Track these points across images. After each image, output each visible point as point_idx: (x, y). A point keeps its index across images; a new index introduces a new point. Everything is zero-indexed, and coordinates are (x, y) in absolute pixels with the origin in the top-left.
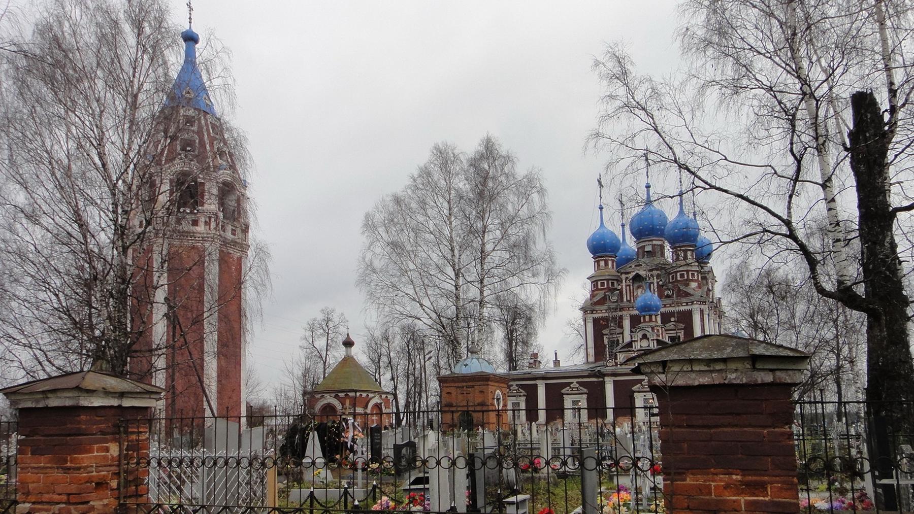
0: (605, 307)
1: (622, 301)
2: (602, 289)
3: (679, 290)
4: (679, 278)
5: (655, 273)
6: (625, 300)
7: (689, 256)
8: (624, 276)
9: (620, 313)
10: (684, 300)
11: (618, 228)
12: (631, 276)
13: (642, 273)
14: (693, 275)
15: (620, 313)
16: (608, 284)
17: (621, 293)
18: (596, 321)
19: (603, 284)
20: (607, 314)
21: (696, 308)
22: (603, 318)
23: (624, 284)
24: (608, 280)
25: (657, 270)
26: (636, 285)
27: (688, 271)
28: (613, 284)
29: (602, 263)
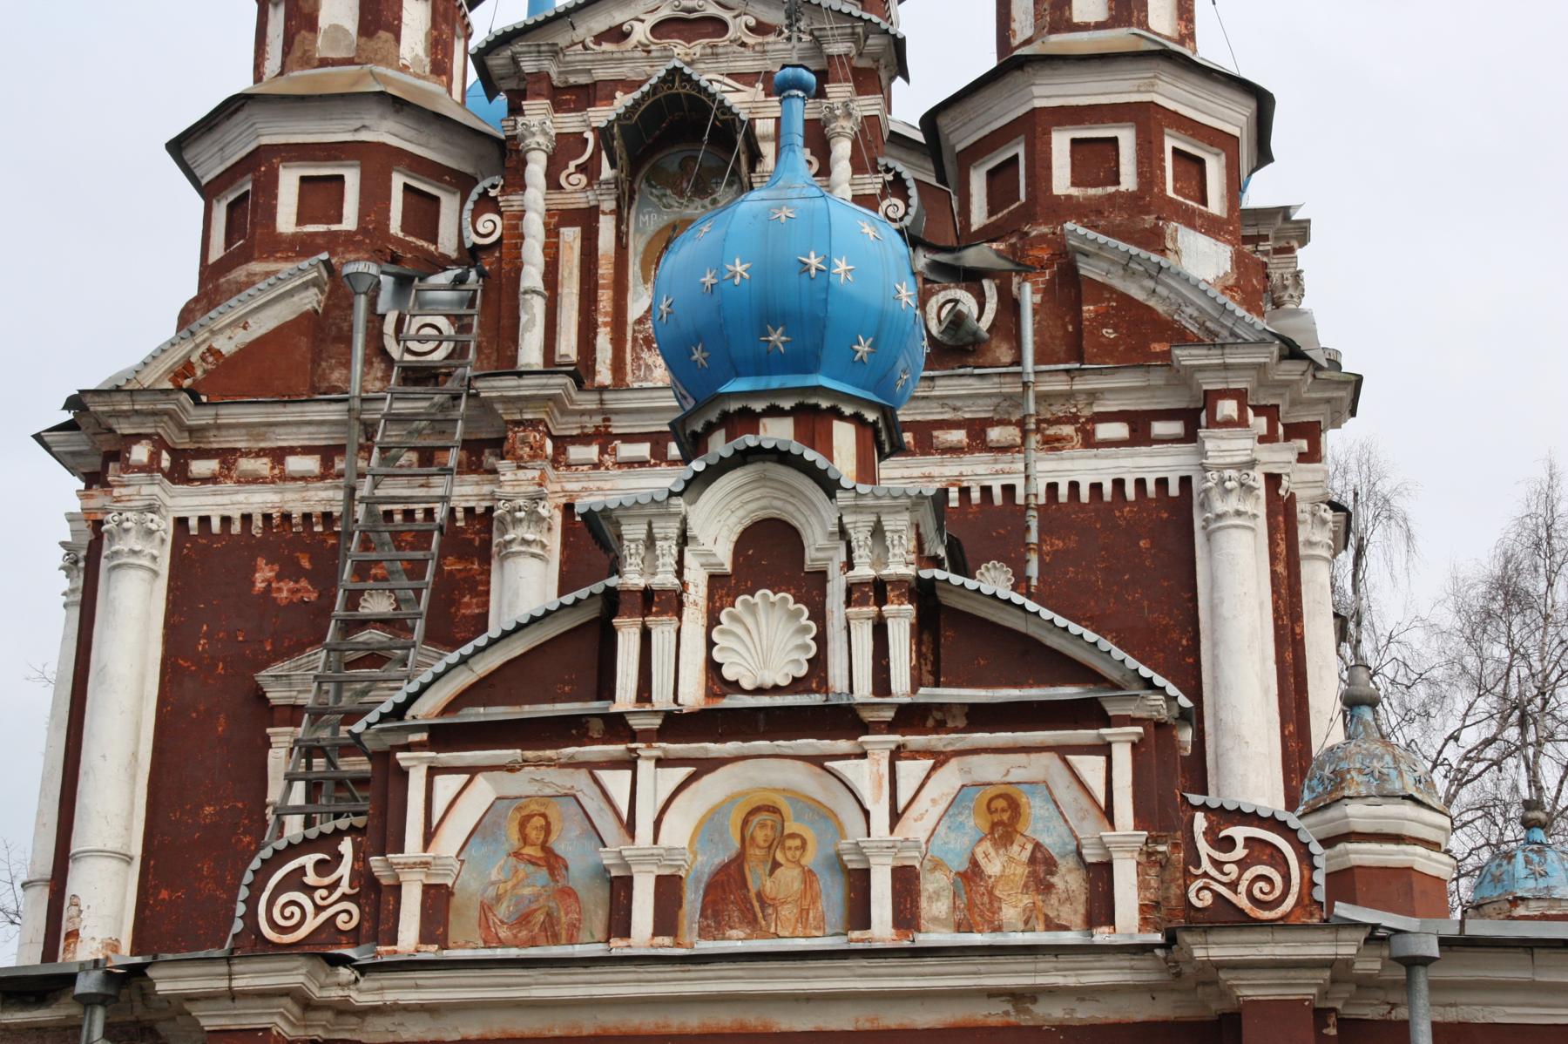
0: (319, 418)
1: (507, 365)
2: (302, 247)
3: (1068, 285)
4: (1061, 181)
6: (530, 352)
9: (467, 492)
10: (1122, 389)
15: (467, 492)
16: (375, 197)
18: (199, 560)
20: (324, 498)
22: (282, 537)
23: (535, 198)
24: (377, 161)
26: (646, 222)
27: (1149, 120)
28: (423, 212)
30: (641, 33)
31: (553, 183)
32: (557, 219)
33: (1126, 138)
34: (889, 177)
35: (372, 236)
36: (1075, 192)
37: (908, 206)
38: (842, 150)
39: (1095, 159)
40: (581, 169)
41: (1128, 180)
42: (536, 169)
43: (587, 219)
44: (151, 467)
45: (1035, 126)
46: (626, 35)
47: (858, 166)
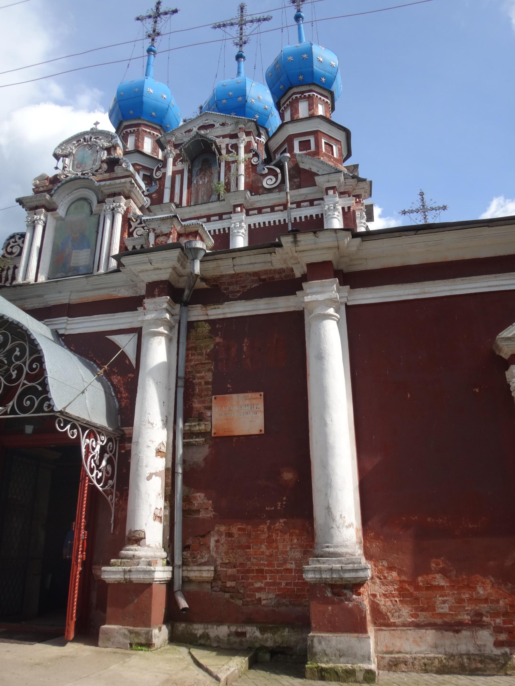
31: (174, 165)
32: (174, 173)
33: (312, 140)
34: (254, 153)
36: (301, 152)
37: (259, 158)
39: (305, 145)
40: (180, 161)
43: (181, 172)
46: (192, 130)
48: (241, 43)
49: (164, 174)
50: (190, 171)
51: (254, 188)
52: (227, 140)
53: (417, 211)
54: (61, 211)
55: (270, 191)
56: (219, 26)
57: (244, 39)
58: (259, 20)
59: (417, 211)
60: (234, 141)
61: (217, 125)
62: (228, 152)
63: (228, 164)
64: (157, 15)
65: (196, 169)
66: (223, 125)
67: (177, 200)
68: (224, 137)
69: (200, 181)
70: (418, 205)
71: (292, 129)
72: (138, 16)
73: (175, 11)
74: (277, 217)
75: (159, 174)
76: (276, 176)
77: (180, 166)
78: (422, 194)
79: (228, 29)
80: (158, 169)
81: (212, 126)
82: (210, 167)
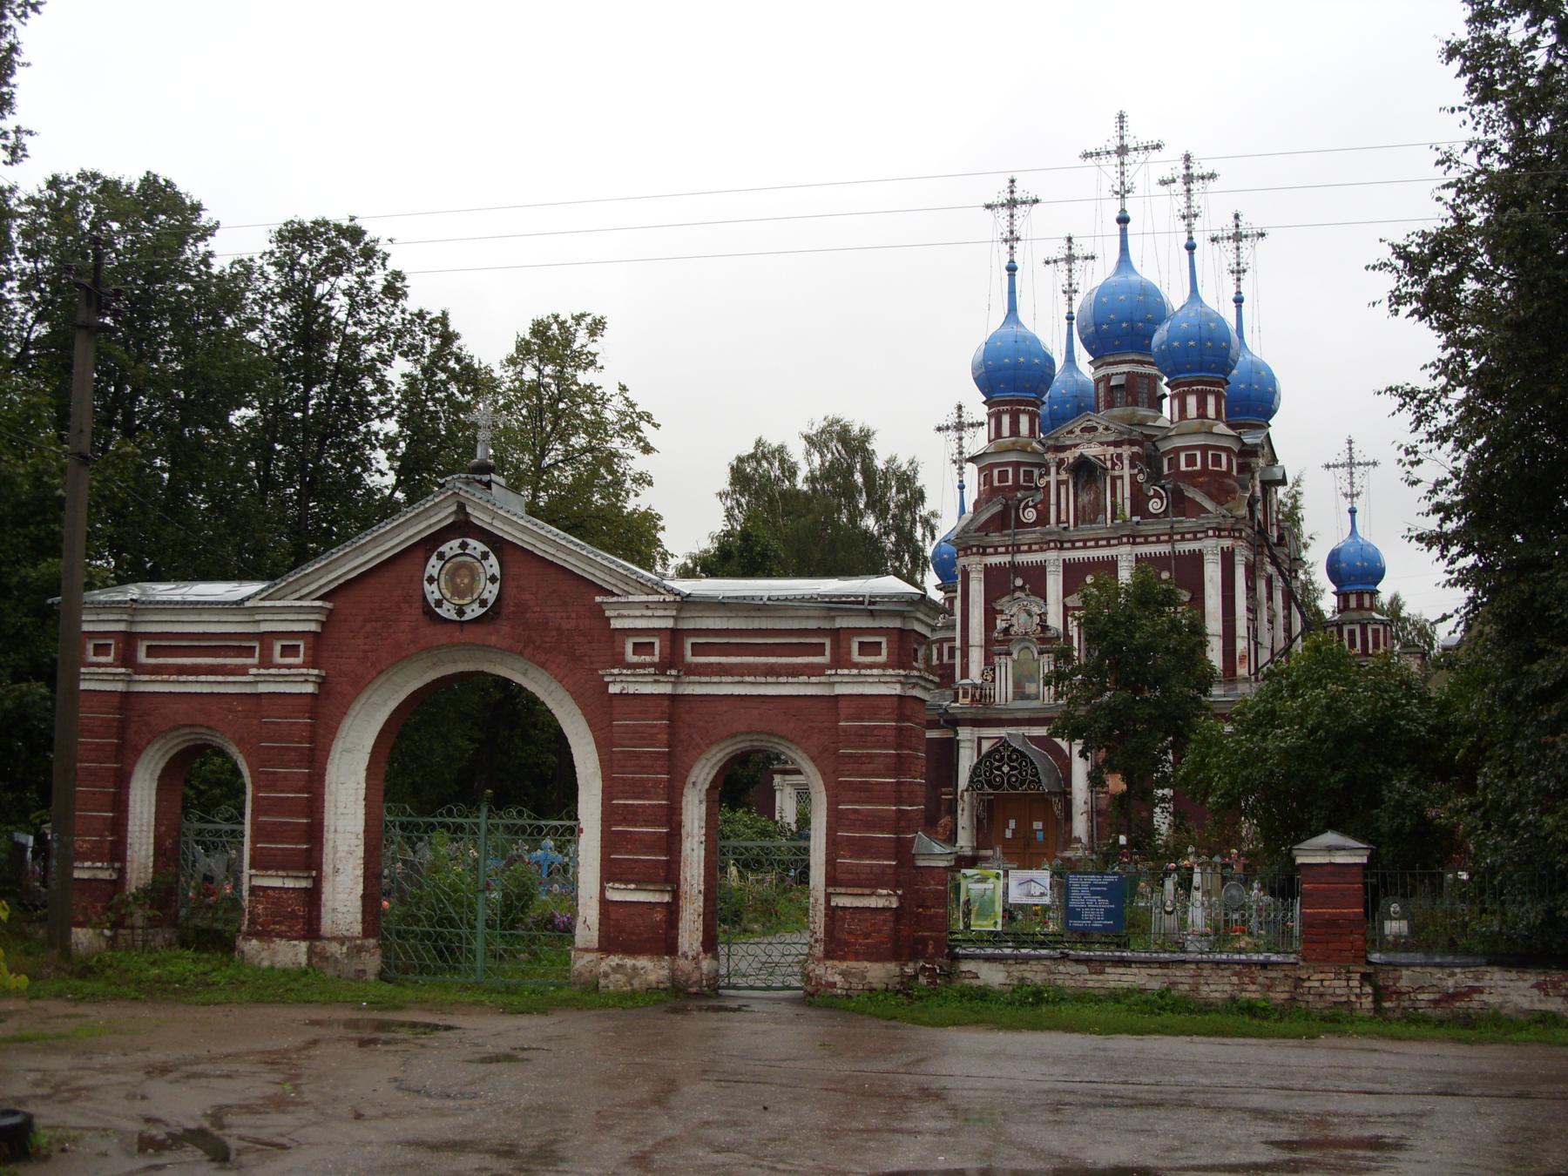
4: (1183, 467)
5: (1126, 451)
7: (1211, 412)
8: (1049, 456)
11: (1050, 329)
12: (1070, 456)
13: (1092, 451)
14: (1217, 460)
17: (1046, 501)
19: (1003, 476)
21: (1212, 549)
23: (1052, 478)
24: (1016, 465)
25: (1132, 443)
27: (1204, 449)
28: (1029, 475)
29: (1006, 420)
30: (1077, 431)
32: (1059, 483)
33: (1198, 454)
35: (1017, 486)
38: (1126, 462)
39: (1191, 460)
41: (1198, 467)
42: (1053, 470)
43: (1066, 482)
44: (977, 553)
45: (1177, 450)
47: (1132, 466)
48: (1123, 193)
49: (1048, 483)
50: (1075, 486)
51: (1139, 505)
52: (1111, 449)
53: (1343, 465)
54: (1015, 656)
55: (1156, 516)
56: (1091, 155)
57: (1128, 185)
58: (1146, 148)
59: (1343, 465)
60: (1119, 450)
61: (1101, 429)
62: (1114, 464)
63: (1114, 479)
64: (1012, 203)
65: (1081, 481)
66: (1107, 429)
67: (1063, 518)
68: (1109, 444)
69: (1085, 498)
70: (1344, 458)
71: (1178, 442)
72: (989, 202)
73: (1036, 201)
74: (1164, 549)
75: (1042, 483)
76: (1161, 499)
77: (1064, 476)
78: (1350, 442)
79: (1103, 160)
80: (1041, 476)
81: (1094, 429)
82: (1095, 481)
